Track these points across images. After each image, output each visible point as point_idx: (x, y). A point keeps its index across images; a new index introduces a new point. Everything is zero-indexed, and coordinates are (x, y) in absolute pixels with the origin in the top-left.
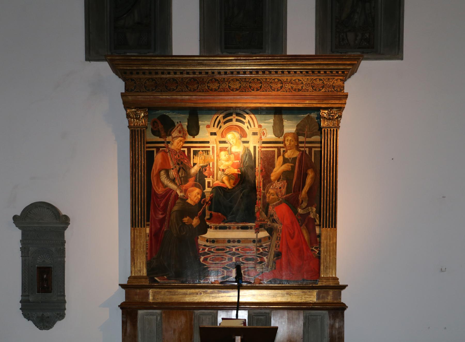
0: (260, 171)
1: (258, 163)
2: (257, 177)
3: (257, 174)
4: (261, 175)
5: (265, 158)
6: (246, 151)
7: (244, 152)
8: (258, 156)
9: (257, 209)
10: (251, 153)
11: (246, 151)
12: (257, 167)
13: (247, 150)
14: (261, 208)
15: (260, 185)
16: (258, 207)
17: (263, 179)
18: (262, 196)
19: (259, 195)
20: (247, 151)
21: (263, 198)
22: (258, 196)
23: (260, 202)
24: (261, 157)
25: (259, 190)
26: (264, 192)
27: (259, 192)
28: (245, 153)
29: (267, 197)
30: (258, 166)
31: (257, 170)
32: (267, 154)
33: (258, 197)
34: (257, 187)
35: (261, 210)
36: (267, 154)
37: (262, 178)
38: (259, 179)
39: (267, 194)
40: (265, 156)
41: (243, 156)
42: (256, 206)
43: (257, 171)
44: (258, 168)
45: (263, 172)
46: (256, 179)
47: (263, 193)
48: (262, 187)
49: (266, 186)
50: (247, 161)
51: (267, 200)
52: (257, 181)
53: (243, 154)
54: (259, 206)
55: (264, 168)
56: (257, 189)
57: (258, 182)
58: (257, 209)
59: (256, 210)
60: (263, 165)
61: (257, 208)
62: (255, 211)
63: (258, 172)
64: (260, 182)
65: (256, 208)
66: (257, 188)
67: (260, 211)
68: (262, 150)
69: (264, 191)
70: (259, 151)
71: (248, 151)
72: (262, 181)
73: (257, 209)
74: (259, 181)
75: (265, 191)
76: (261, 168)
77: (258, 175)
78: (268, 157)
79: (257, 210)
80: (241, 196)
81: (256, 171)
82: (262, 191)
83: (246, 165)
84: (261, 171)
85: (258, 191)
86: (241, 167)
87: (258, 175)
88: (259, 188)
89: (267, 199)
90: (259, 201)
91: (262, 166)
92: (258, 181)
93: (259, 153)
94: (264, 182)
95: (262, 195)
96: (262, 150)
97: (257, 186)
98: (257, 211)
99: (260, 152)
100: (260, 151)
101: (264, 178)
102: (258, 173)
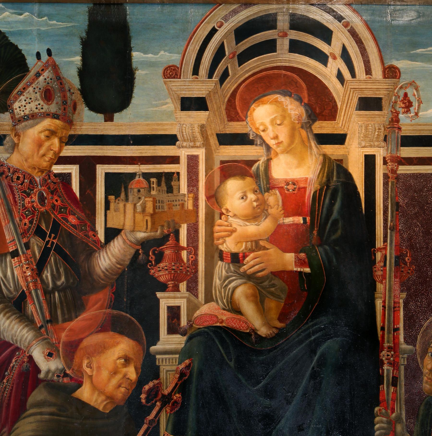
0: (393, 261)
1: (385, 227)
2: (380, 287)
3: (380, 273)
4: (396, 277)
5: (414, 207)
6: (335, 179)
7: (325, 179)
8: (385, 200)
9: (382, 422)
10: (355, 187)
11: (335, 179)
12: (379, 243)
13: (338, 173)
14: (398, 419)
15: (396, 321)
16: (387, 416)
17: (404, 295)
18: (402, 368)
19: (390, 364)
20: (338, 177)
21: (406, 377)
22: (385, 367)
23: (395, 392)
24: (398, 204)
25: (388, 342)
26: (411, 351)
27: (390, 349)
28: (328, 187)
29: (425, 371)
30: (385, 241)
31: (379, 256)
32: (421, 190)
33: (388, 370)
34: (383, 329)
35: (399, 428)
36: (421, 190)
37: (402, 291)
38: (390, 297)
39: (423, 358)
40: (412, 199)
41: (320, 195)
42: (377, 409)
43: (379, 264)
44: (385, 249)
45: (405, 264)
46: (376, 295)
47: (406, 356)
48: (402, 331)
49: (422, 326)
50: (335, 222)
51: (424, 384)
52: (379, 303)
53: (321, 190)
54: (393, 412)
55: (411, 247)
56: (380, 339)
57: (384, 307)
58: (382, 422)
59: (377, 426)
60: (405, 236)
61: (384, 419)
62: (375, 432)
63: (382, 264)
64: (395, 309)
65: (377, 419)
66: (380, 333)
67: (394, 431)
68: (398, 172)
69: (410, 347)
70: (386, 176)
71: (342, 175)
72: (401, 301)
73: (383, 425)
74: (389, 302)
75: (415, 346)
76: (398, 248)
77: (385, 278)
78: (428, 203)
79: (383, 428)
80: (313, 368)
81: (374, 262)
82: (404, 346)
83: (333, 237)
84: (396, 261)
85: (386, 345)
86: (313, 246)
87: (384, 277)
88: (389, 333)
89: (425, 378)
90: (392, 389)
91: (402, 238)
92: (384, 302)
93: (386, 184)
94: (412, 306)
95: (403, 362)
96: (398, 172)
97: (379, 323)
98: (382, 431)
99: (390, 180)
100: (390, 175)
101: (408, 289)
102: (384, 271)
